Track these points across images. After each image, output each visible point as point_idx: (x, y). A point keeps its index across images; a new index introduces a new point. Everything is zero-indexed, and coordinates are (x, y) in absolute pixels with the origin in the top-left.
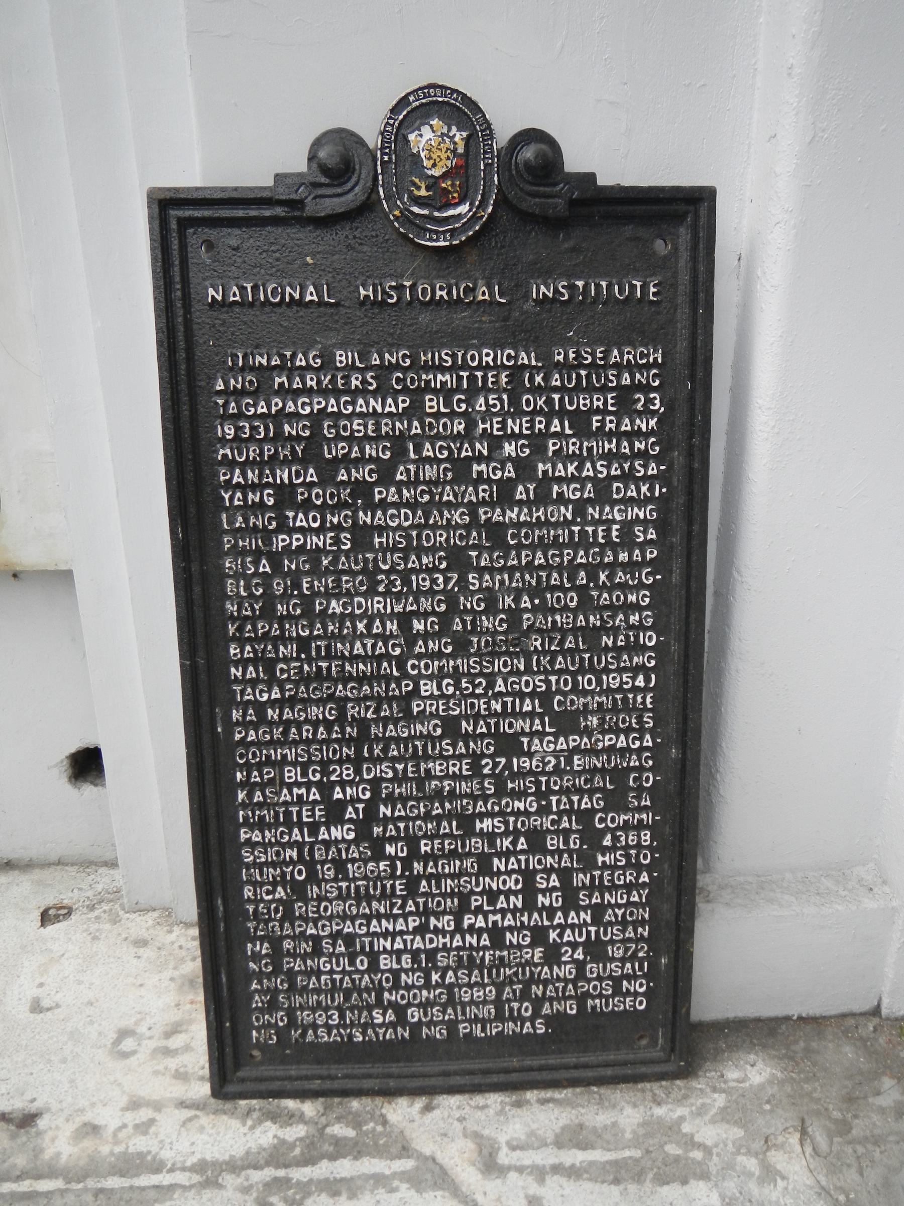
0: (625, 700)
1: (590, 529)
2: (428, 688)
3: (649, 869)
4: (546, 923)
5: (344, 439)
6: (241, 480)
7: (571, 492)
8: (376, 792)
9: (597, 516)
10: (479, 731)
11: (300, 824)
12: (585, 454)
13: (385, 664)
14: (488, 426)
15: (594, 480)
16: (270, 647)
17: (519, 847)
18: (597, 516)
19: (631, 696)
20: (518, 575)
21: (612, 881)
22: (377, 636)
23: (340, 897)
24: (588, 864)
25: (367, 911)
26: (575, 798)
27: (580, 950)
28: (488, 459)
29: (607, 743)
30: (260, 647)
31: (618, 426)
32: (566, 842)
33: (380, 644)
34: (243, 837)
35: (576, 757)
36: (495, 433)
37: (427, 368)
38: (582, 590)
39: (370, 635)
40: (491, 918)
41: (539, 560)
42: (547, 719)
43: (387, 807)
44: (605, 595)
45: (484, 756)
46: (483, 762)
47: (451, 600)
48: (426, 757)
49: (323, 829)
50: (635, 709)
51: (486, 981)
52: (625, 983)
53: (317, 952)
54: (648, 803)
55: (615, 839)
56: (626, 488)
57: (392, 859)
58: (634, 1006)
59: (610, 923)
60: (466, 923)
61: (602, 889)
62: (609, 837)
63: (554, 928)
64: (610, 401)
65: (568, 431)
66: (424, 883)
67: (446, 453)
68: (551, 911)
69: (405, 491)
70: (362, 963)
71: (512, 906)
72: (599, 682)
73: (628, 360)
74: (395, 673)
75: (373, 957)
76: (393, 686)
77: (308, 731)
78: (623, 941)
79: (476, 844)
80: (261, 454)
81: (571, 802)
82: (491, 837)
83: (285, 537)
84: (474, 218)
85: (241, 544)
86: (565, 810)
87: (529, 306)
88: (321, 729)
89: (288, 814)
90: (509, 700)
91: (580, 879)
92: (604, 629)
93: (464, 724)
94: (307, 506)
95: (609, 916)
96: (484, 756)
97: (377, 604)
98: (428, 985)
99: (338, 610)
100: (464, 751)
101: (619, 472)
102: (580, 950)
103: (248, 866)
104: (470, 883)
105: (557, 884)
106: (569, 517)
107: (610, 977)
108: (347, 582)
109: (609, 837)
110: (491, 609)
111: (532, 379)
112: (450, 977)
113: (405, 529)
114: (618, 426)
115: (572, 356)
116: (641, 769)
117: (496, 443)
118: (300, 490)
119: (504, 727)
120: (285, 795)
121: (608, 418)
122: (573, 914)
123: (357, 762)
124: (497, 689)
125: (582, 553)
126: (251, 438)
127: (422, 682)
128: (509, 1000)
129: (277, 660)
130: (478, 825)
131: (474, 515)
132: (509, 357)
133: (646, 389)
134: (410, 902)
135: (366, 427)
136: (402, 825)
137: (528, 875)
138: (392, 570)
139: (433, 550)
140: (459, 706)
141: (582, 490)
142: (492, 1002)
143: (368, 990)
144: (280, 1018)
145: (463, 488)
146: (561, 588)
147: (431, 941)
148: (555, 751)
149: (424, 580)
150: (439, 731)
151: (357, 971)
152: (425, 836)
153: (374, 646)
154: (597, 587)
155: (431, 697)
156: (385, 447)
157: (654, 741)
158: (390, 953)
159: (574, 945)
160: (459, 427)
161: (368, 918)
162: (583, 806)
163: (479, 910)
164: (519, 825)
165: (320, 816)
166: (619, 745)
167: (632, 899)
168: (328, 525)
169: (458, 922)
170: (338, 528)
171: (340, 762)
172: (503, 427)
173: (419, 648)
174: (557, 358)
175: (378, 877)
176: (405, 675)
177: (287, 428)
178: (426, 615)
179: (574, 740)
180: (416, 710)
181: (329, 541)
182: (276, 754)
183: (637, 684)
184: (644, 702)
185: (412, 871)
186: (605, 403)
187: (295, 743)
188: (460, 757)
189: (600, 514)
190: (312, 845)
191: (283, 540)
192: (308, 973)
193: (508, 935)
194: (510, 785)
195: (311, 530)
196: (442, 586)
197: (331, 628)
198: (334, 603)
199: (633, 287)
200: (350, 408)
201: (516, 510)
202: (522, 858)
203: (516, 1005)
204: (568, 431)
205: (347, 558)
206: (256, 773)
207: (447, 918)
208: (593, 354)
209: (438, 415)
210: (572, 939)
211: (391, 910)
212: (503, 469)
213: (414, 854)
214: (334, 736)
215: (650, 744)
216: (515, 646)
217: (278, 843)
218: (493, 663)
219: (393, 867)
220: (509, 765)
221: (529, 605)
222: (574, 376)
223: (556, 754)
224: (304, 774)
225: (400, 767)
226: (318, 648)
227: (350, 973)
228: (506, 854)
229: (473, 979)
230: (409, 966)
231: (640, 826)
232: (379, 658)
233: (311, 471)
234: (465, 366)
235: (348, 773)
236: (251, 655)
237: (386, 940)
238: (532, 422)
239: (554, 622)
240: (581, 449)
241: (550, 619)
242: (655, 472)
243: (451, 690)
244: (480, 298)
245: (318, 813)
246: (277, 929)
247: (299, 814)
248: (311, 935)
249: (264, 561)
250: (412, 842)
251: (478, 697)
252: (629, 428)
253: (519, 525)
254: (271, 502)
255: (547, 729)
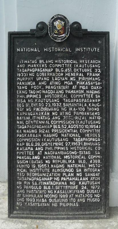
0: (94, 131)
1: (87, 95)
2: (55, 127)
3: (100, 168)
4: (79, 180)
5: (40, 76)
6: (21, 84)
7: (83, 88)
8: (44, 148)
9: (88, 93)
10: (65, 136)
11: (29, 155)
12: (86, 80)
13: (47, 121)
14: (67, 74)
15: (87, 85)
16: (25, 117)
17: (73, 162)
18: (88, 93)
19: (95, 130)
20: (73, 104)
21: (92, 171)
22: (45, 116)
23: (36, 172)
24: (87, 167)
25: (42, 175)
26: (84, 152)
27: (86, 187)
28: (67, 81)
29: (91, 140)
30: (23, 118)
31: (92, 75)
32: (83, 162)
33: (46, 117)
34: (18, 158)
35: (84, 143)
36: (69, 76)
37: (56, 63)
38: (86, 108)
39: (44, 115)
40: (67, 178)
41: (77, 101)
42: (79, 134)
43: (46, 152)
44: (90, 108)
45: (66, 142)
46: (66, 143)
47: (60, 109)
48: (54, 142)
49: (33, 156)
50: (96, 133)
51: (66, 193)
52: (95, 195)
53: (31, 184)
54: (99, 154)
55: (93, 161)
56: (94, 87)
57: (47, 164)
58: (97, 201)
59: (92, 181)
60: (62, 179)
61: (90, 173)
62: (91, 161)
63: (80, 181)
64: (91, 70)
65: (83, 76)
66: (53, 169)
67: (59, 79)
68: (79, 177)
69: (51, 87)
70: (40, 188)
71: (71, 176)
72: (89, 127)
73: (94, 63)
74: (49, 123)
75: (42, 186)
76: (48, 126)
77: (31, 135)
78: (94, 185)
79: (64, 161)
80: (25, 79)
81: (84, 153)
82: (67, 160)
83: (29, 95)
84: (65, 37)
85: (20, 96)
86: (82, 155)
87: (75, 52)
88: (34, 135)
89: (27, 153)
90: (71, 130)
91: (85, 170)
92: (90, 116)
93: (62, 134)
94: (33, 89)
95: (91, 179)
96: (66, 142)
97: (46, 109)
98: (54, 194)
99: (38, 110)
100: (62, 140)
101: (92, 84)
102: (86, 187)
103: (18, 164)
104: (63, 170)
105: (81, 171)
106: (83, 92)
107: (92, 193)
108: (40, 104)
109: (91, 161)
110: (68, 110)
111: (76, 66)
112: (58, 192)
113: (51, 94)
114: (92, 75)
115: (83, 61)
116: (97, 146)
117: (69, 78)
118: (32, 86)
119: (70, 136)
120: (26, 149)
121: (90, 73)
122: (84, 178)
123: (41, 142)
124: (69, 127)
125: (85, 100)
126: (23, 76)
127: (54, 125)
128: (70, 198)
129: (26, 120)
130: (65, 157)
131: (65, 92)
132: (72, 62)
133: (97, 68)
134: (50, 174)
135: (45, 74)
136: (49, 156)
137: (75, 169)
138: (49, 102)
139: (56, 99)
140: (61, 131)
141: (86, 87)
142: (67, 198)
143: (41, 194)
144: (22, 200)
145: (62, 86)
146: (81, 107)
147: (55, 183)
148: (80, 141)
149: (55, 104)
150: (57, 136)
151: (39, 189)
152: (54, 159)
153: (45, 118)
154: (88, 107)
155: (56, 129)
156: (48, 78)
157: (100, 140)
158: (46, 185)
159: (84, 185)
160: (62, 74)
161: (42, 177)
162: (86, 154)
163: (64, 176)
164: (73, 157)
165: (33, 154)
166: (93, 140)
167: (96, 175)
168: (37, 93)
169: (60, 179)
170: (39, 94)
171: (37, 142)
172: (70, 75)
173: (53, 118)
174: (81, 62)
175: (44, 168)
176: (51, 124)
177: (30, 74)
178: (55, 111)
179: (84, 139)
180: (52, 131)
181: (37, 96)
182: (25, 140)
183: (97, 127)
184: (98, 131)
185: (51, 167)
186: (90, 71)
187: (29, 138)
188: (61, 142)
189: (89, 92)
190: (31, 160)
191: (28, 96)
192: (29, 189)
193: (71, 182)
194: (71, 148)
195: (33, 94)
196: (58, 106)
197: (37, 114)
198: (37, 108)
199: (95, 49)
200: (42, 71)
201: (73, 91)
202: (74, 165)
203: (72, 199)
204: (83, 76)
205: (40, 100)
206: (21, 144)
207: (58, 178)
208: (87, 61)
209: (58, 72)
210: (84, 184)
211: (47, 175)
212: (70, 83)
213: (51, 163)
214: (36, 136)
215: (100, 140)
216: (72, 118)
217: (24, 159)
218: (68, 122)
219: (47, 166)
220: (71, 144)
221: (75, 110)
222: (84, 65)
223: (81, 142)
224: (30, 144)
225: (49, 144)
226: (34, 118)
227: (38, 190)
228: (70, 164)
229: (63, 193)
230: (50, 189)
231: (98, 159)
232: (46, 120)
233: (34, 82)
234: (63, 63)
235: (39, 144)
236: (21, 119)
237: (45, 182)
238: (76, 74)
239: (80, 114)
240: (85, 79)
241: (79, 113)
242: (99, 84)
243: (60, 127)
244: (66, 51)
245: (33, 153)
246: (23, 179)
247: (29, 153)
248: (30, 180)
249: (24, 100)
250: (51, 160)
251: (65, 129)
252: (94, 75)
253: (73, 94)
254: (26, 88)
255: (79, 136)
